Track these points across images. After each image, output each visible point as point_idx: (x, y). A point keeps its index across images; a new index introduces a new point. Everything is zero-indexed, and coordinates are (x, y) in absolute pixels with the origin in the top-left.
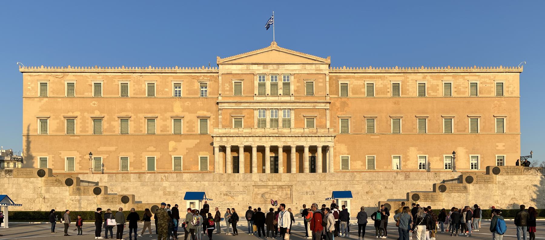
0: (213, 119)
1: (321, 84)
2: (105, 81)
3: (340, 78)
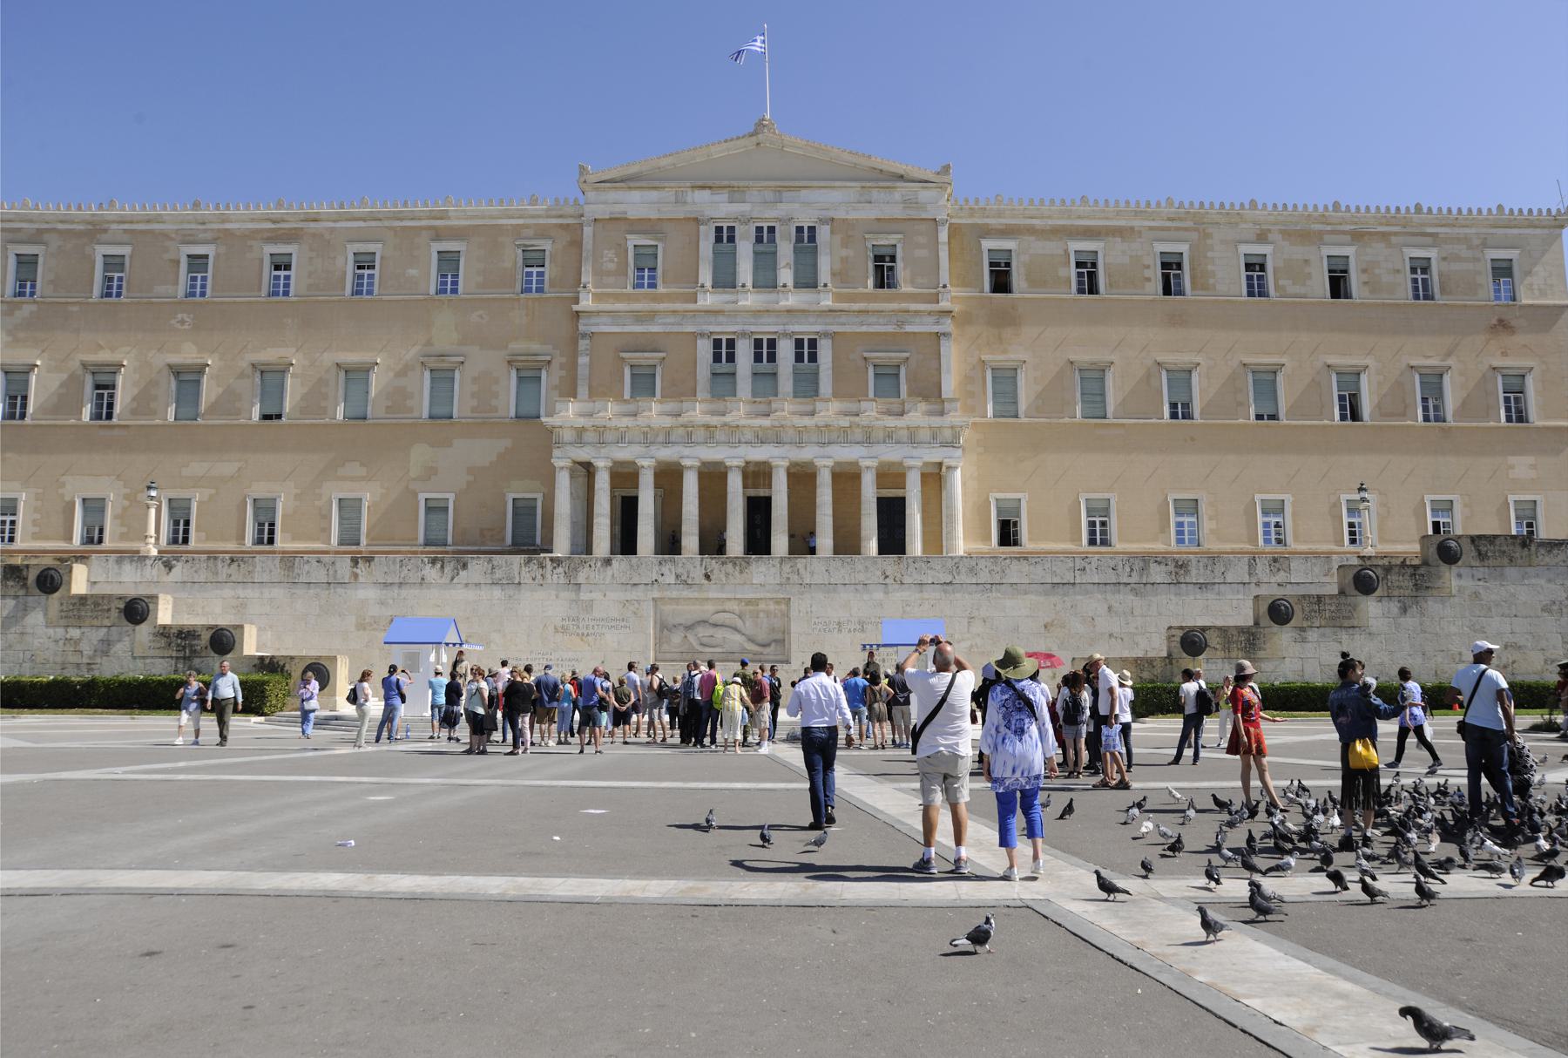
0: (561, 368)
1: (922, 253)
2: (222, 249)
3: (986, 232)
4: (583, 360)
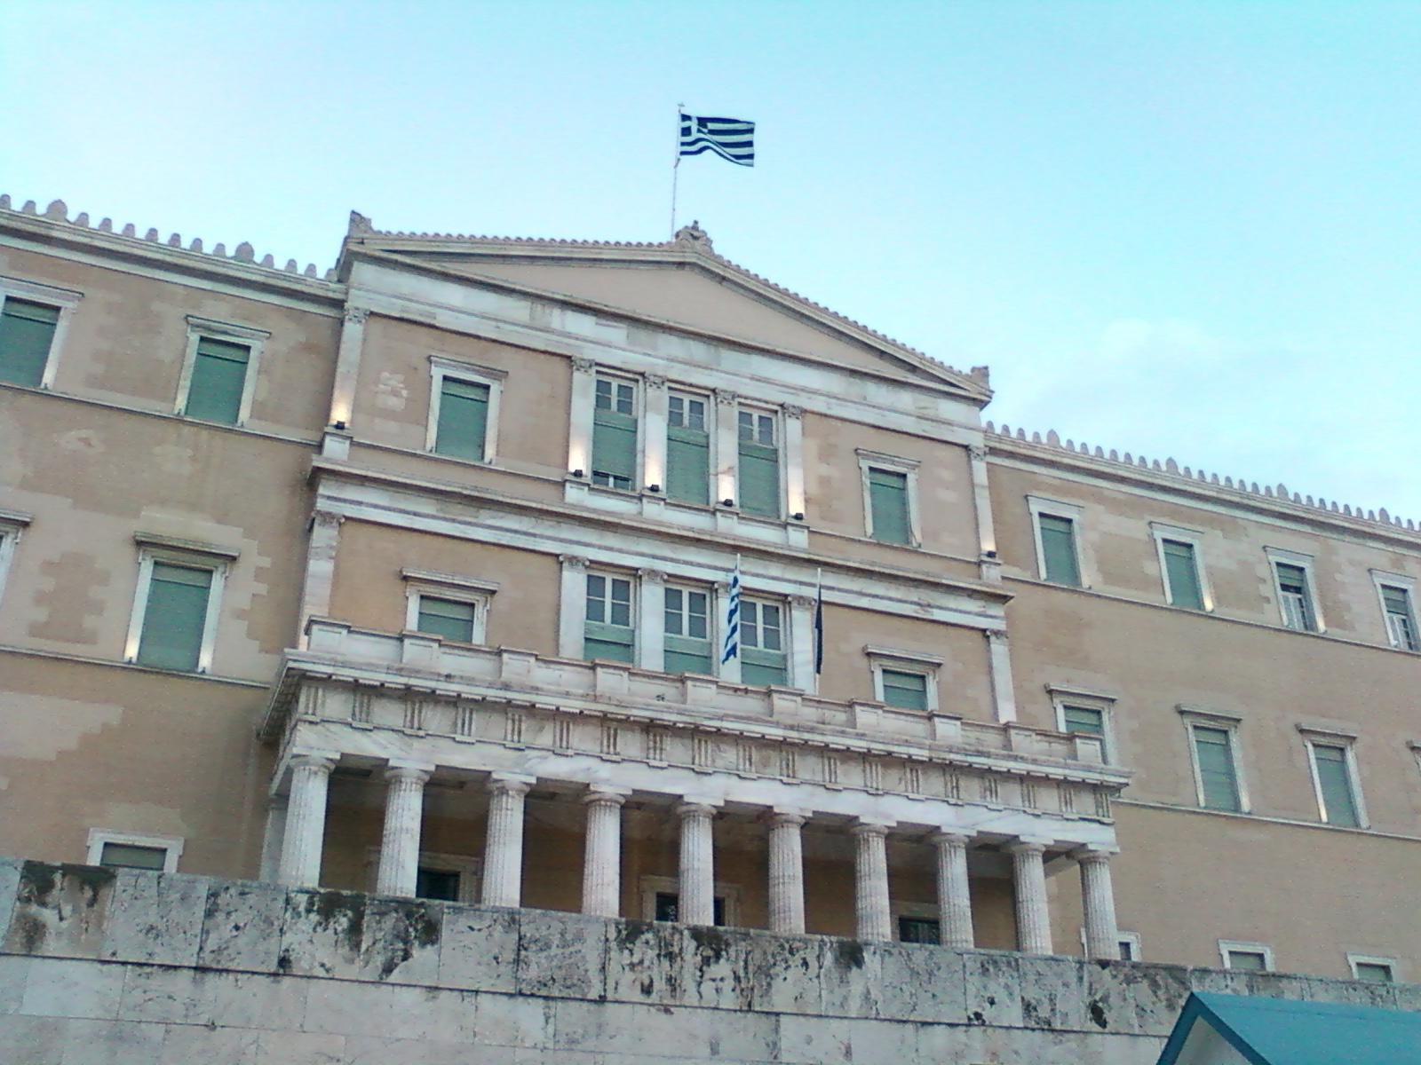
0: (260, 574)
1: (948, 496)
4: (320, 568)
